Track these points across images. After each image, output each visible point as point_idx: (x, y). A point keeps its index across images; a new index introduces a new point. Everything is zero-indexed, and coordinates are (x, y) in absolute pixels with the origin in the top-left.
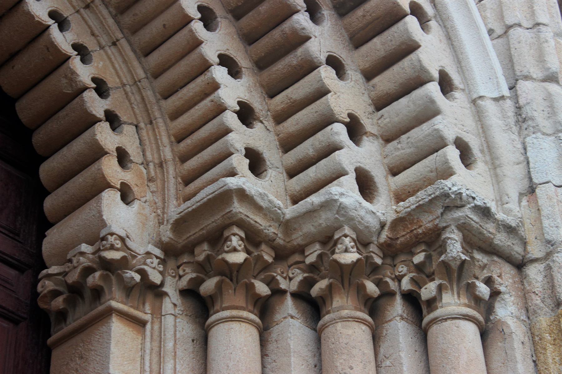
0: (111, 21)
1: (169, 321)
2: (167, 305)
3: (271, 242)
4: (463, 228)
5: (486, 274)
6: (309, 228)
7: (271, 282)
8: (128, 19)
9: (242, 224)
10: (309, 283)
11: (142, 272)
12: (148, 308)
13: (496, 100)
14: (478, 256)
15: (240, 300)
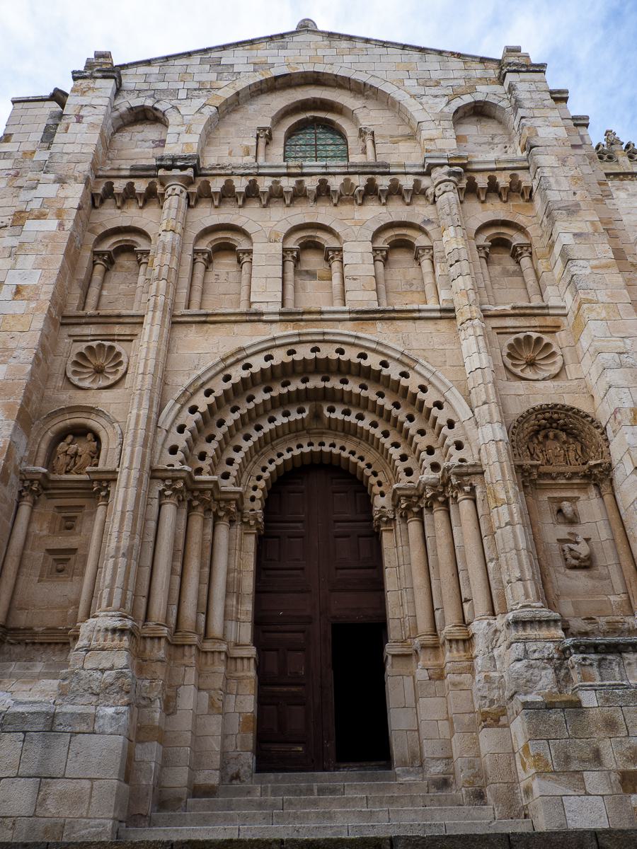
0: (366, 445)
1: (398, 527)
2: (397, 522)
3: (415, 495)
4: (455, 474)
5: (470, 482)
6: (421, 488)
7: (419, 506)
8: (369, 442)
9: (403, 496)
10: (427, 502)
11: (388, 517)
12: (393, 525)
14: (465, 478)
15: (412, 515)
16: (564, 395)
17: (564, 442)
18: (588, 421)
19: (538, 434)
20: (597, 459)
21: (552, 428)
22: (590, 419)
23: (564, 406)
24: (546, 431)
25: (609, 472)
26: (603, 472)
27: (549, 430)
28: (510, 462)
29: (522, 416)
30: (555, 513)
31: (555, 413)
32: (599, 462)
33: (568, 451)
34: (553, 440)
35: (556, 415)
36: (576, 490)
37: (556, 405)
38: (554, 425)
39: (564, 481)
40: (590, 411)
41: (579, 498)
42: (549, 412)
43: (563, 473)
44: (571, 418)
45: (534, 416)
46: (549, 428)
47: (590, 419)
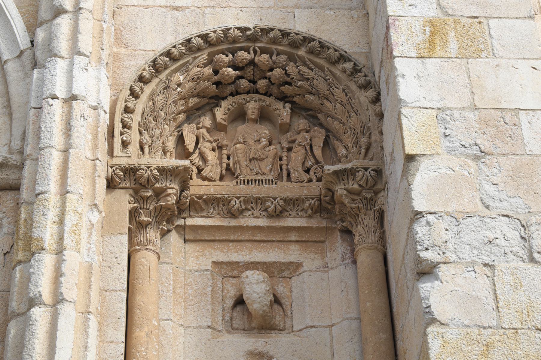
13: (19, 56)
16: (297, 12)
17: (285, 129)
18: (344, 71)
19: (218, 105)
20: (350, 161)
21: (257, 92)
22: (348, 66)
23: (285, 34)
24: (239, 99)
25: (376, 193)
26: (358, 194)
27: (246, 96)
28: (94, 153)
29: (168, 54)
30: (230, 303)
31: (264, 51)
32: (349, 166)
33: (290, 149)
34: (255, 121)
35: (265, 56)
36: (295, 247)
37: (266, 31)
38: (262, 83)
39: (262, 222)
40: (355, 49)
41: (299, 265)
42: (247, 50)
43: (259, 201)
44: (305, 64)
45: (203, 57)
46: (248, 93)
47: (348, 66)
